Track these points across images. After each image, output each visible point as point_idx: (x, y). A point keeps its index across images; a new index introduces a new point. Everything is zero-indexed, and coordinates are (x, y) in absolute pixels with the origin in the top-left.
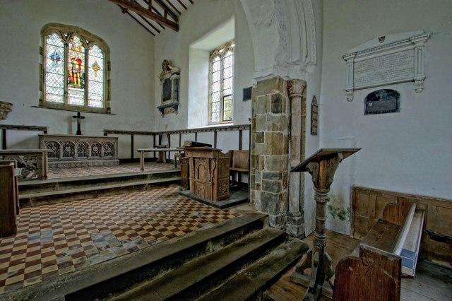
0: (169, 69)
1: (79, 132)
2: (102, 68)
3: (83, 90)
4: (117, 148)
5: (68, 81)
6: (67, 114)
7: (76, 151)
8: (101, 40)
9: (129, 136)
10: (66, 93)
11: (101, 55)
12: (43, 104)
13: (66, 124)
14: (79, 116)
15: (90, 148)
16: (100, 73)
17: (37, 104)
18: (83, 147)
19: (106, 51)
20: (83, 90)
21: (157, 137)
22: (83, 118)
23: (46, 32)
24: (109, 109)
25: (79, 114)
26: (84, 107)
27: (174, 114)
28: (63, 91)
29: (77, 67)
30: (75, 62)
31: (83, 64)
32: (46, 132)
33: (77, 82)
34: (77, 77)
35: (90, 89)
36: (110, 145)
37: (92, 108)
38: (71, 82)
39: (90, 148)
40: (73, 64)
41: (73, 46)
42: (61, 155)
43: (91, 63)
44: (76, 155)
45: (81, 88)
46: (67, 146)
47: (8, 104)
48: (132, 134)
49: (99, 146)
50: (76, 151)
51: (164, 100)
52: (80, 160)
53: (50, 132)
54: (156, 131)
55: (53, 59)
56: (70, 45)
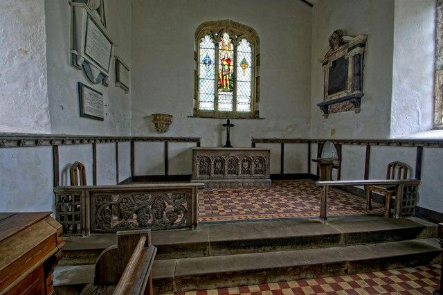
0: (342, 43)
1: (228, 144)
2: (250, 65)
3: (231, 93)
4: (269, 163)
5: (219, 86)
6: (216, 122)
7: (226, 167)
8: (251, 30)
9: (279, 145)
10: (216, 98)
11: (250, 48)
12: (198, 114)
13: (216, 134)
14: (229, 125)
15: (240, 163)
16: (248, 70)
17: (192, 113)
18: (234, 162)
19: (255, 43)
20: (231, 93)
21: (315, 147)
22: (232, 125)
23: (199, 37)
24: (257, 112)
25: (228, 121)
26: (232, 112)
27: (352, 112)
28: (213, 97)
29: (226, 67)
30: (225, 63)
31: (232, 64)
32: (199, 145)
33: (226, 85)
34: (226, 80)
35: (239, 92)
36: (262, 160)
37: (241, 113)
38: (221, 86)
39: (240, 163)
40: (222, 65)
41: (223, 45)
42: (212, 172)
43: (239, 60)
44: (226, 172)
45: (230, 91)
46: (217, 161)
47: (169, 116)
48: (282, 142)
49: (249, 161)
50: (226, 167)
51: (330, 93)
52: (230, 178)
53: (203, 144)
54: (312, 137)
55: (205, 63)
56: (220, 44)
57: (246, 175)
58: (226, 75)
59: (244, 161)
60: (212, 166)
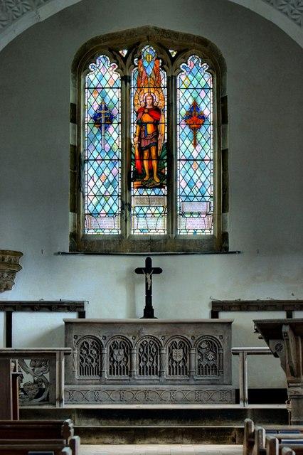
1: (149, 312)
3: (164, 191)
7: (135, 360)
8: (204, 42)
10: (126, 206)
11: (207, 77)
15: (165, 351)
30: (147, 118)
31: (164, 119)
32: (82, 315)
44: (136, 370)
49: (185, 346)
50: (135, 360)
57: (178, 377)
58: (148, 148)
59: (175, 346)
60: (106, 358)
